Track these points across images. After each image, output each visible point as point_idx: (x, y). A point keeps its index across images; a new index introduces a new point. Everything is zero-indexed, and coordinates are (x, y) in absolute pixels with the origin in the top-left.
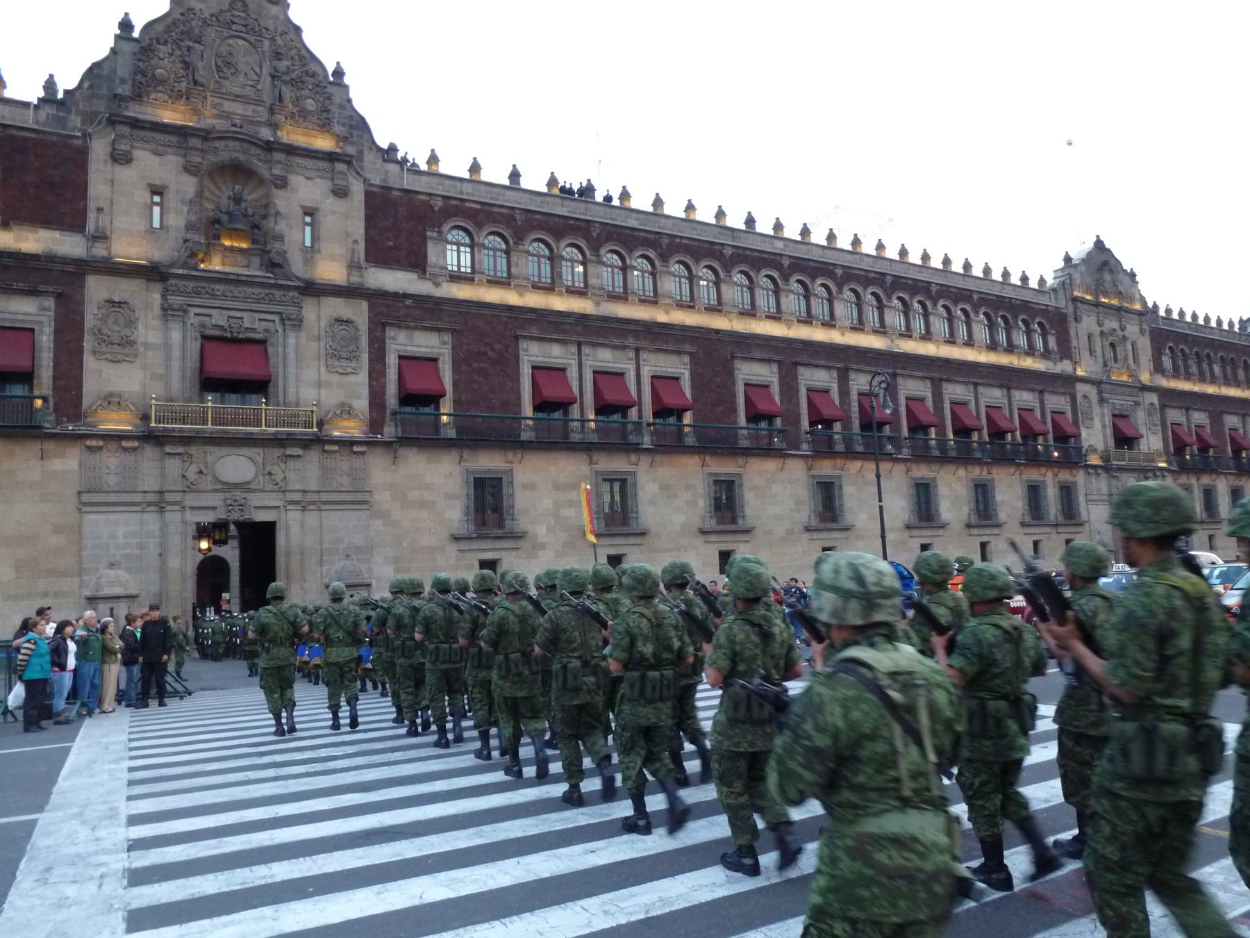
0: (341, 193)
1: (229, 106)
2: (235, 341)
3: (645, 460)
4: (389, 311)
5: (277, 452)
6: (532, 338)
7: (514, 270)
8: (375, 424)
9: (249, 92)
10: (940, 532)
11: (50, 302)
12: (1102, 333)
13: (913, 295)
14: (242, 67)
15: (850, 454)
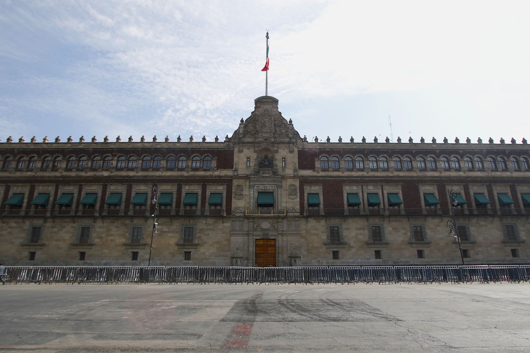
0: (291, 152)
1: (264, 135)
2: (266, 192)
3: (386, 221)
4: (304, 181)
5: (276, 220)
6: (347, 185)
7: (341, 166)
8: (302, 212)
9: (268, 130)
10: (522, 245)
11: (225, 187)
13: (496, 156)
14: (267, 125)
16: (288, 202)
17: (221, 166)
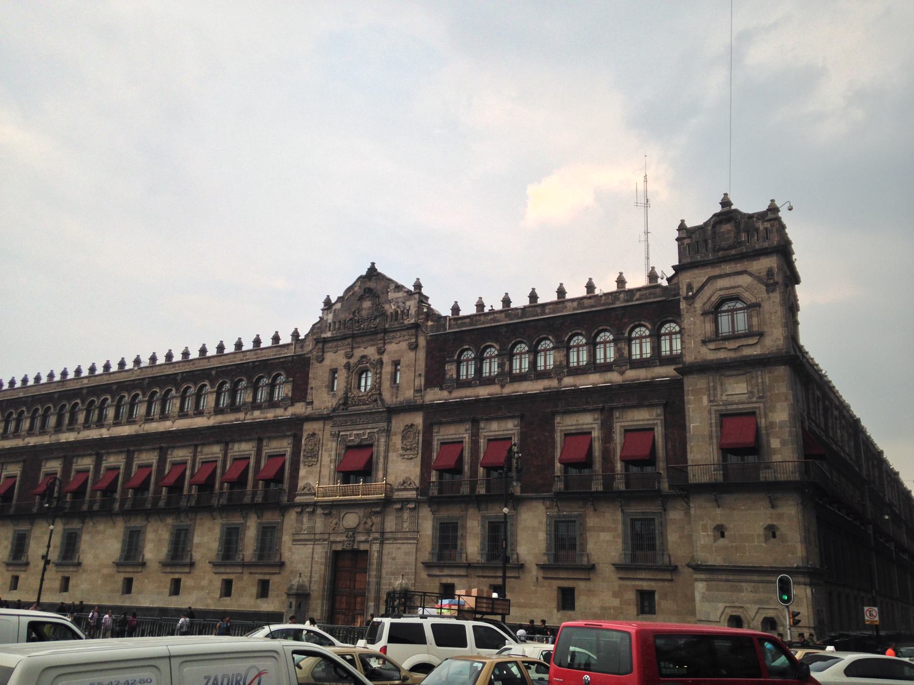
12: (348, 366)
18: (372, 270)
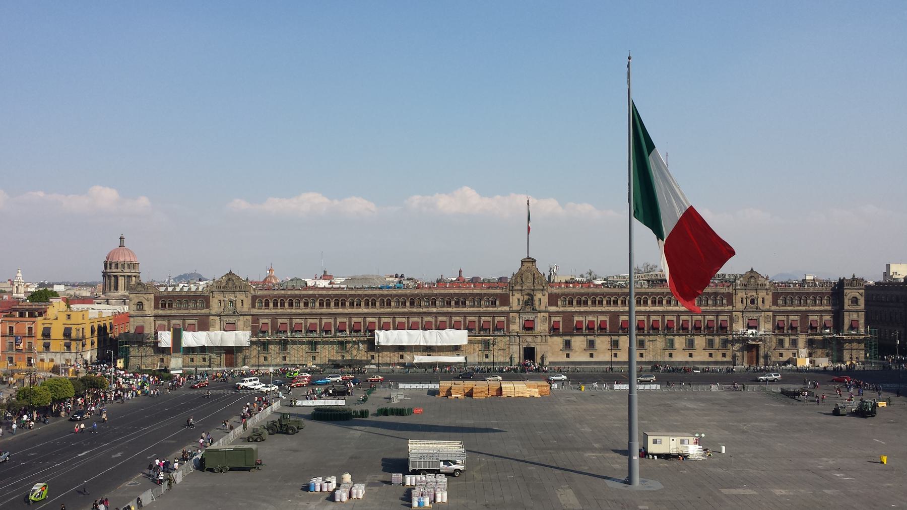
4: (551, 314)
15: (649, 334)
16: (541, 326)
17: (502, 304)
18: (752, 270)
